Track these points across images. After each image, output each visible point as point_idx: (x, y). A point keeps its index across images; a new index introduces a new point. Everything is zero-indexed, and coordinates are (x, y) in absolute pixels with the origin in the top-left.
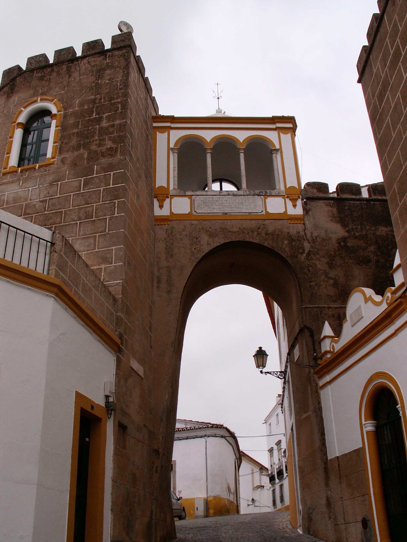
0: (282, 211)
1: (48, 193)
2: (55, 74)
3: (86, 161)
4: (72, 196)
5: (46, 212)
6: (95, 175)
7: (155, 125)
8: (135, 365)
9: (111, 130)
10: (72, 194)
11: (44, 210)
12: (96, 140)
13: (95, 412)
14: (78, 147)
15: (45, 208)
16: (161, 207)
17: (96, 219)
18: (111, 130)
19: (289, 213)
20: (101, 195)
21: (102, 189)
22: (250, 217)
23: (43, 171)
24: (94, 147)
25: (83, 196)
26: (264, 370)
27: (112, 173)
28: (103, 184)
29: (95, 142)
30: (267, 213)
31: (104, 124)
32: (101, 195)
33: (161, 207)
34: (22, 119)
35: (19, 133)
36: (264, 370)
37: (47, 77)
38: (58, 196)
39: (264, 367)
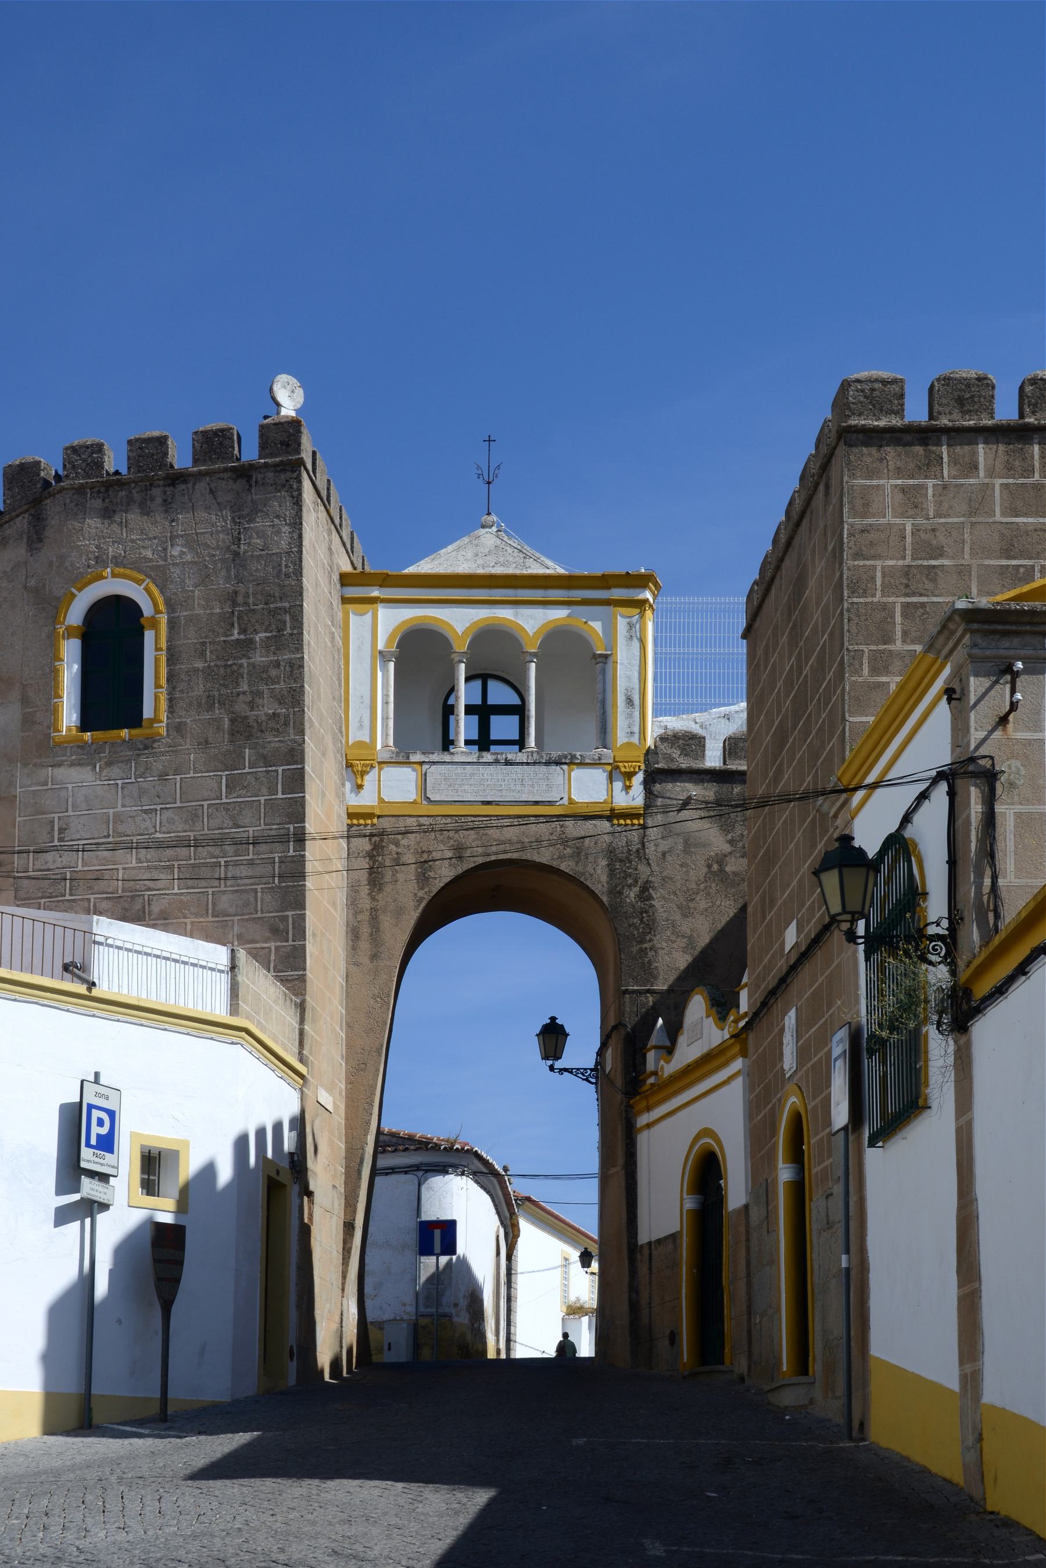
1: (159, 797)
3: (226, 736)
4: (206, 807)
5: (158, 835)
6: (247, 770)
10: (205, 803)
11: (153, 830)
12: (244, 693)
15: (155, 827)
17: (255, 857)
20: (262, 810)
21: (262, 799)
23: (141, 747)
25: (227, 810)
27: (280, 769)
28: (264, 790)
29: (242, 698)
32: (262, 810)
38: (179, 804)
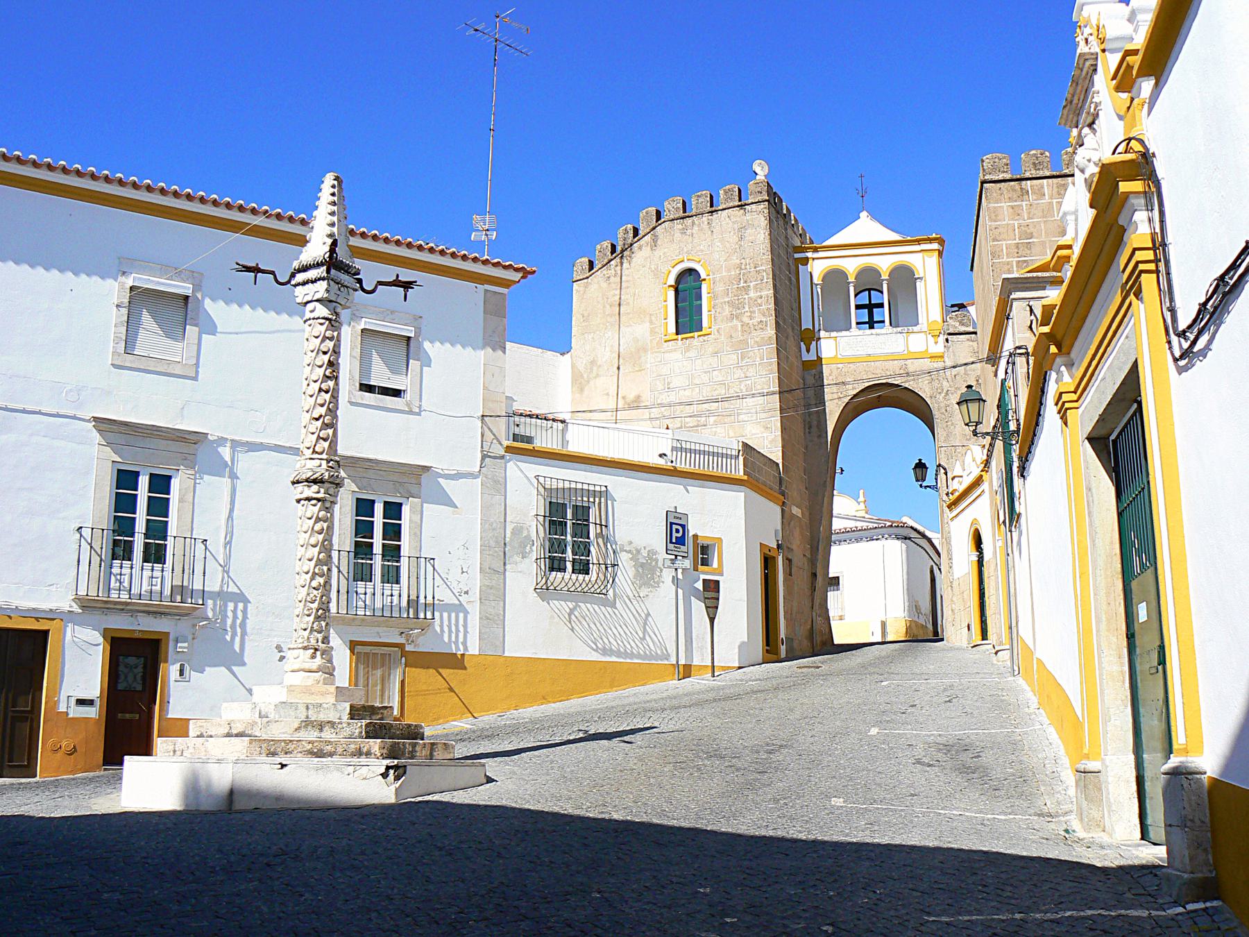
0: (923, 349)
2: (696, 228)
7: (796, 256)
8: (796, 511)
9: (759, 301)
13: (772, 554)
14: (732, 316)
16: (808, 351)
18: (759, 301)
19: (930, 351)
22: (892, 358)
24: (746, 320)
26: (925, 484)
30: (910, 352)
31: (752, 294)
33: (808, 351)
34: (672, 281)
35: (671, 294)
36: (925, 484)
37: (689, 232)
39: (924, 480)
